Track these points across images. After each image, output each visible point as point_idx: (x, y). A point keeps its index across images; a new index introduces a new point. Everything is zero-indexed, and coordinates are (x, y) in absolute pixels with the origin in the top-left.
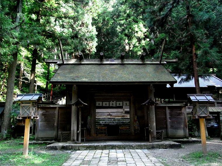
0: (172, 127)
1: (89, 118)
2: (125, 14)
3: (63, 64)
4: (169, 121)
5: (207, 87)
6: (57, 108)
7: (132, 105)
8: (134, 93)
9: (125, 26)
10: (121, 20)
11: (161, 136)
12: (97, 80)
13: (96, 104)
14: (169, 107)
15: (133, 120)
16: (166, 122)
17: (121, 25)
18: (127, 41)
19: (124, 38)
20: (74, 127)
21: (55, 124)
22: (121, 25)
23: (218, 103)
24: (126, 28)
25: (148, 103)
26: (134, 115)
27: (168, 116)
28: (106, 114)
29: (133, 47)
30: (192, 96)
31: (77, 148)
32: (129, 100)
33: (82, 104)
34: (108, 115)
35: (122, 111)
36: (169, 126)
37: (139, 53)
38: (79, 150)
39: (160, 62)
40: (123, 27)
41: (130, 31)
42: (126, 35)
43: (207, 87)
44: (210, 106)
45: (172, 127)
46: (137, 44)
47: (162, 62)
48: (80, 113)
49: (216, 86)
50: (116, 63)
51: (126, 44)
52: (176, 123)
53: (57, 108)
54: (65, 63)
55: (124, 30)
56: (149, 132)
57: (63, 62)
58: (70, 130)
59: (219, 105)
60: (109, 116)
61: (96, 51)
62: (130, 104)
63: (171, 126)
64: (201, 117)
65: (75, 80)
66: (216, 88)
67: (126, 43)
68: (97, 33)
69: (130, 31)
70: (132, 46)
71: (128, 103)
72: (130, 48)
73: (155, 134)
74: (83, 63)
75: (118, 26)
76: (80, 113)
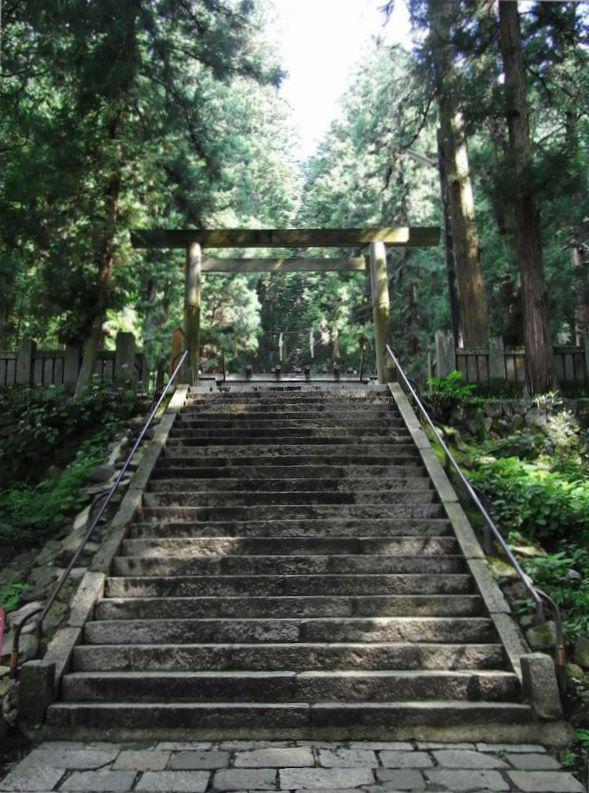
3: (224, 381)
9: (321, 288)
10: (312, 276)
17: (312, 287)
18: (324, 322)
19: (320, 314)
22: (312, 287)
24: (324, 292)
29: (339, 336)
37: (351, 350)
40: (316, 292)
41: (332, 297)
42: (324, 307)
46: (346, 330)
47: (364, 379)
51: (324, 330)
54: (227, 379)
55: (317, 298)
61: (257, 345)
67: (324, 326)
69: (332, 297)
70: (336, 333)
72: (331, 336)
75: (306, 290)
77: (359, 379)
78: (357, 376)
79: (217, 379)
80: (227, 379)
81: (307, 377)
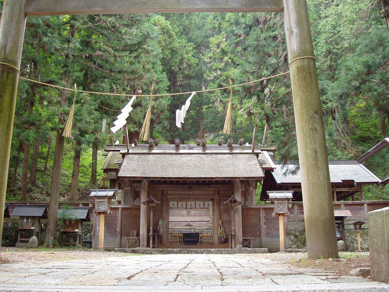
0: (267, 234)
1: (161, 222)
2: (218, 47)
4: (264, 227)
5: (342, 182)
6: (120, 209)
7: (216, 207)
8: (219, 190)
11: (250, 243)
12: (172, 176)
13: (169, 205)
14: (265, 209)
15: (216, 225)
16: (260, 228)
20: (143, 231)
21: (118, 229)
23: (346, 205)
25: (231, 201)
26: (218, 219)
27: (263, 221)
28: (184, 217)
30: (271, 192)
31: (149, 252)
32: (212, 200)
33: (153, 202)
34: (186, 226)
35: (209, 219)
36: (263, 234)
38: (151, 254)
39: (253, 151)
43: (342, 182)
44: (336, 209)
45: (267, 234)
47: (256, 151)
48: (152, 213)
49: (356, 181)
50: (198, 152)
52: (272, 229)
53: (120, 209)
54: (130, 152)
56: (233, 236)
57: (128, 151)
58: (138, 235)
59: (348, 207)
60: (188, 227)
62: (213, 204)
63: (266, 233)
64: (280, 214)
65: (146, 174)
66: (355, 184)
68: (168, 84)
71: (211, 203)
73: (241, 239)
74: (153, 151)
76: (152, 213)
77: (251, 151)
78: (249, 148)
79: (121, 152)
80: (130, 152)
81: (204, 150)
